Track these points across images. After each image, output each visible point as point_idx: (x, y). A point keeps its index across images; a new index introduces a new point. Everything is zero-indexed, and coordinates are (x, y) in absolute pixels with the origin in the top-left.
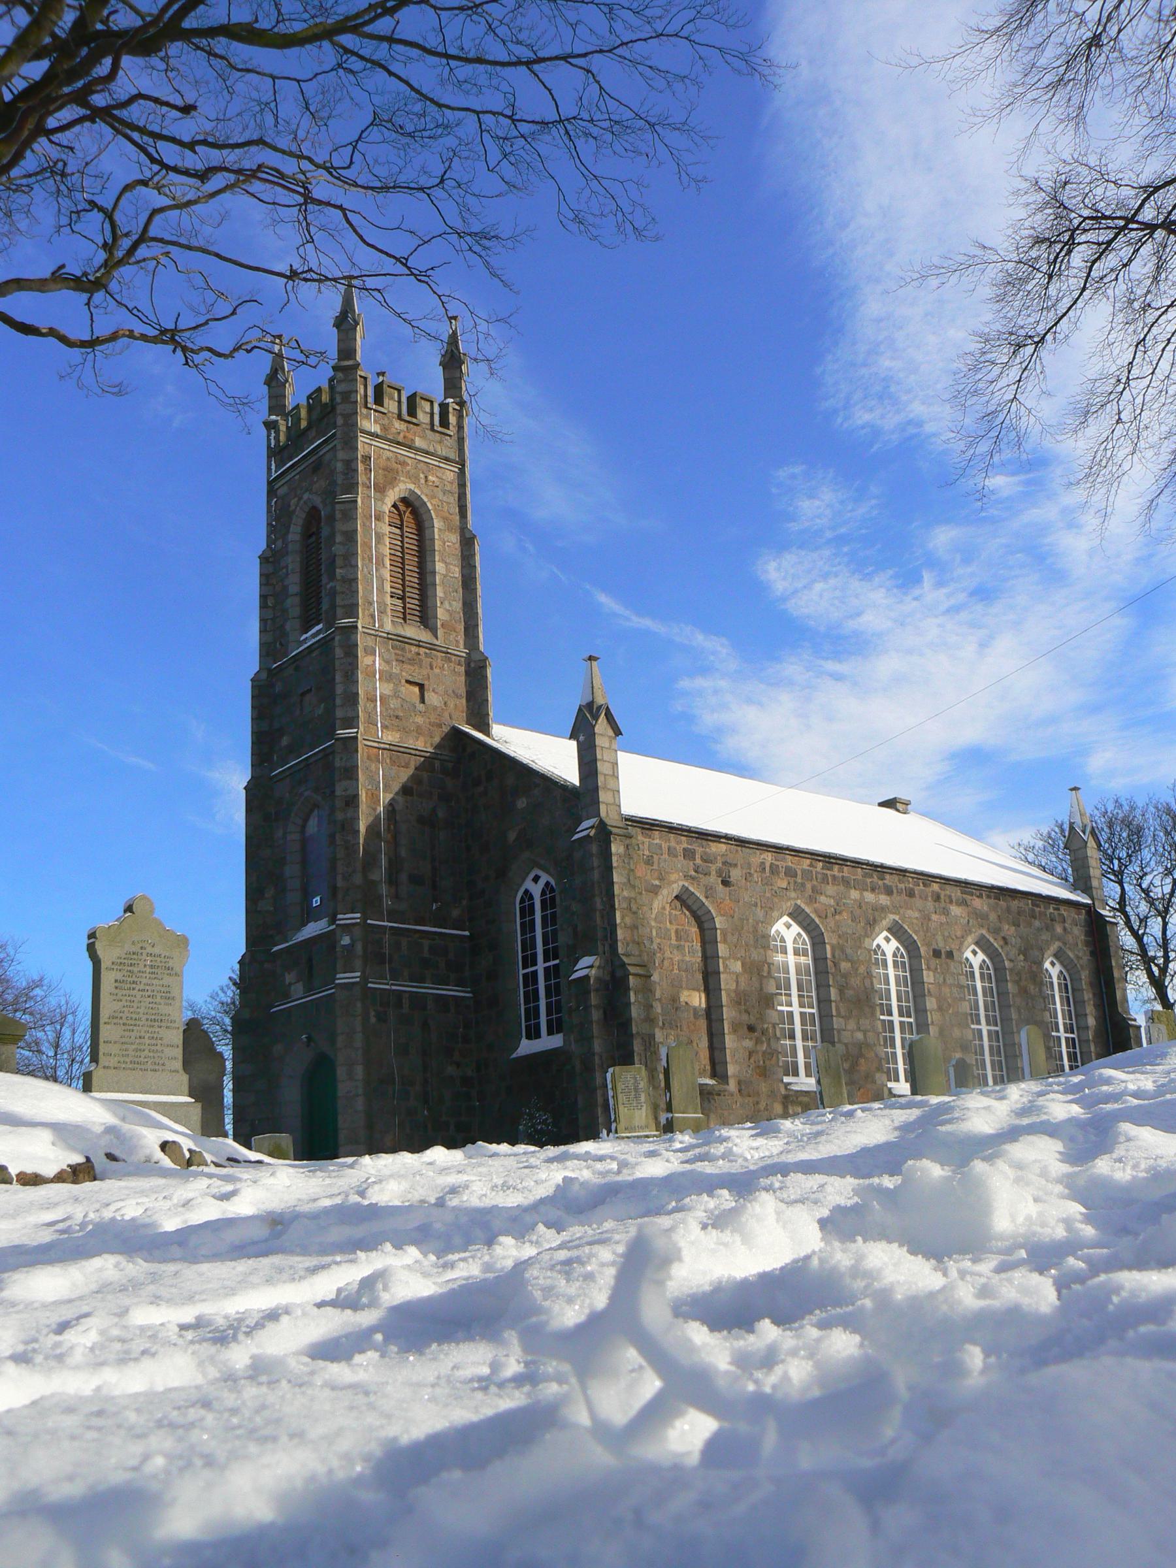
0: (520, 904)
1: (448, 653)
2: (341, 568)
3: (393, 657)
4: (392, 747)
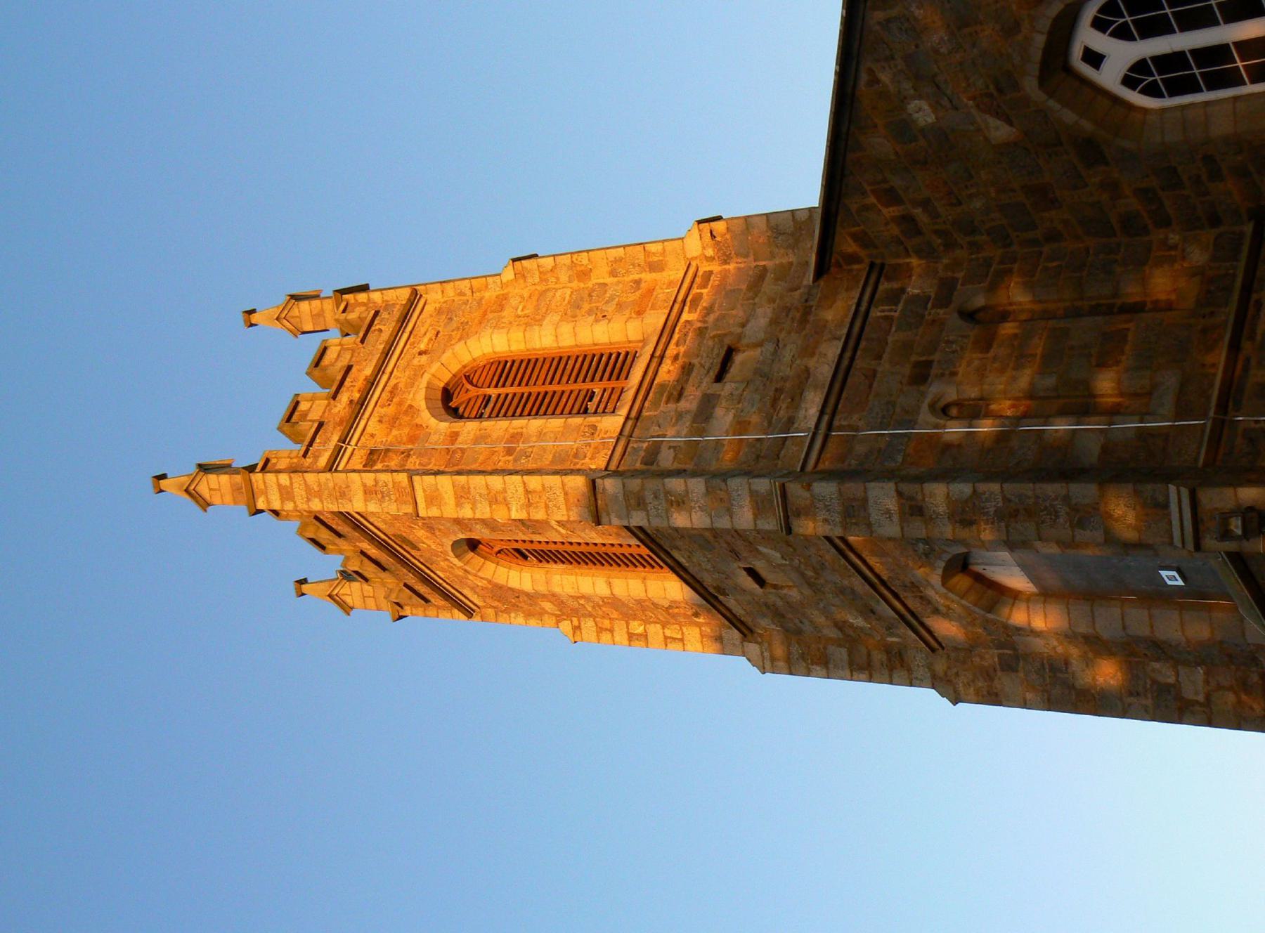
0: (1161, 96)
1: (684, 302)
2: (509, 509)
3: (672, 406)
4: (829, 410)
